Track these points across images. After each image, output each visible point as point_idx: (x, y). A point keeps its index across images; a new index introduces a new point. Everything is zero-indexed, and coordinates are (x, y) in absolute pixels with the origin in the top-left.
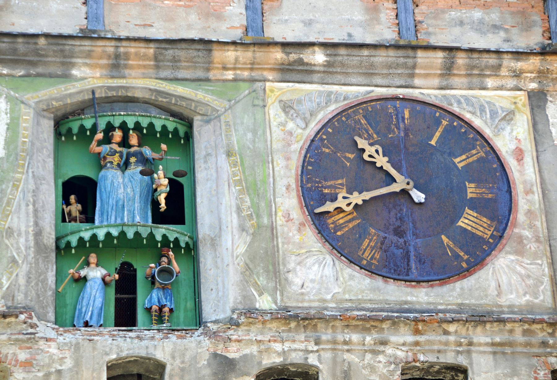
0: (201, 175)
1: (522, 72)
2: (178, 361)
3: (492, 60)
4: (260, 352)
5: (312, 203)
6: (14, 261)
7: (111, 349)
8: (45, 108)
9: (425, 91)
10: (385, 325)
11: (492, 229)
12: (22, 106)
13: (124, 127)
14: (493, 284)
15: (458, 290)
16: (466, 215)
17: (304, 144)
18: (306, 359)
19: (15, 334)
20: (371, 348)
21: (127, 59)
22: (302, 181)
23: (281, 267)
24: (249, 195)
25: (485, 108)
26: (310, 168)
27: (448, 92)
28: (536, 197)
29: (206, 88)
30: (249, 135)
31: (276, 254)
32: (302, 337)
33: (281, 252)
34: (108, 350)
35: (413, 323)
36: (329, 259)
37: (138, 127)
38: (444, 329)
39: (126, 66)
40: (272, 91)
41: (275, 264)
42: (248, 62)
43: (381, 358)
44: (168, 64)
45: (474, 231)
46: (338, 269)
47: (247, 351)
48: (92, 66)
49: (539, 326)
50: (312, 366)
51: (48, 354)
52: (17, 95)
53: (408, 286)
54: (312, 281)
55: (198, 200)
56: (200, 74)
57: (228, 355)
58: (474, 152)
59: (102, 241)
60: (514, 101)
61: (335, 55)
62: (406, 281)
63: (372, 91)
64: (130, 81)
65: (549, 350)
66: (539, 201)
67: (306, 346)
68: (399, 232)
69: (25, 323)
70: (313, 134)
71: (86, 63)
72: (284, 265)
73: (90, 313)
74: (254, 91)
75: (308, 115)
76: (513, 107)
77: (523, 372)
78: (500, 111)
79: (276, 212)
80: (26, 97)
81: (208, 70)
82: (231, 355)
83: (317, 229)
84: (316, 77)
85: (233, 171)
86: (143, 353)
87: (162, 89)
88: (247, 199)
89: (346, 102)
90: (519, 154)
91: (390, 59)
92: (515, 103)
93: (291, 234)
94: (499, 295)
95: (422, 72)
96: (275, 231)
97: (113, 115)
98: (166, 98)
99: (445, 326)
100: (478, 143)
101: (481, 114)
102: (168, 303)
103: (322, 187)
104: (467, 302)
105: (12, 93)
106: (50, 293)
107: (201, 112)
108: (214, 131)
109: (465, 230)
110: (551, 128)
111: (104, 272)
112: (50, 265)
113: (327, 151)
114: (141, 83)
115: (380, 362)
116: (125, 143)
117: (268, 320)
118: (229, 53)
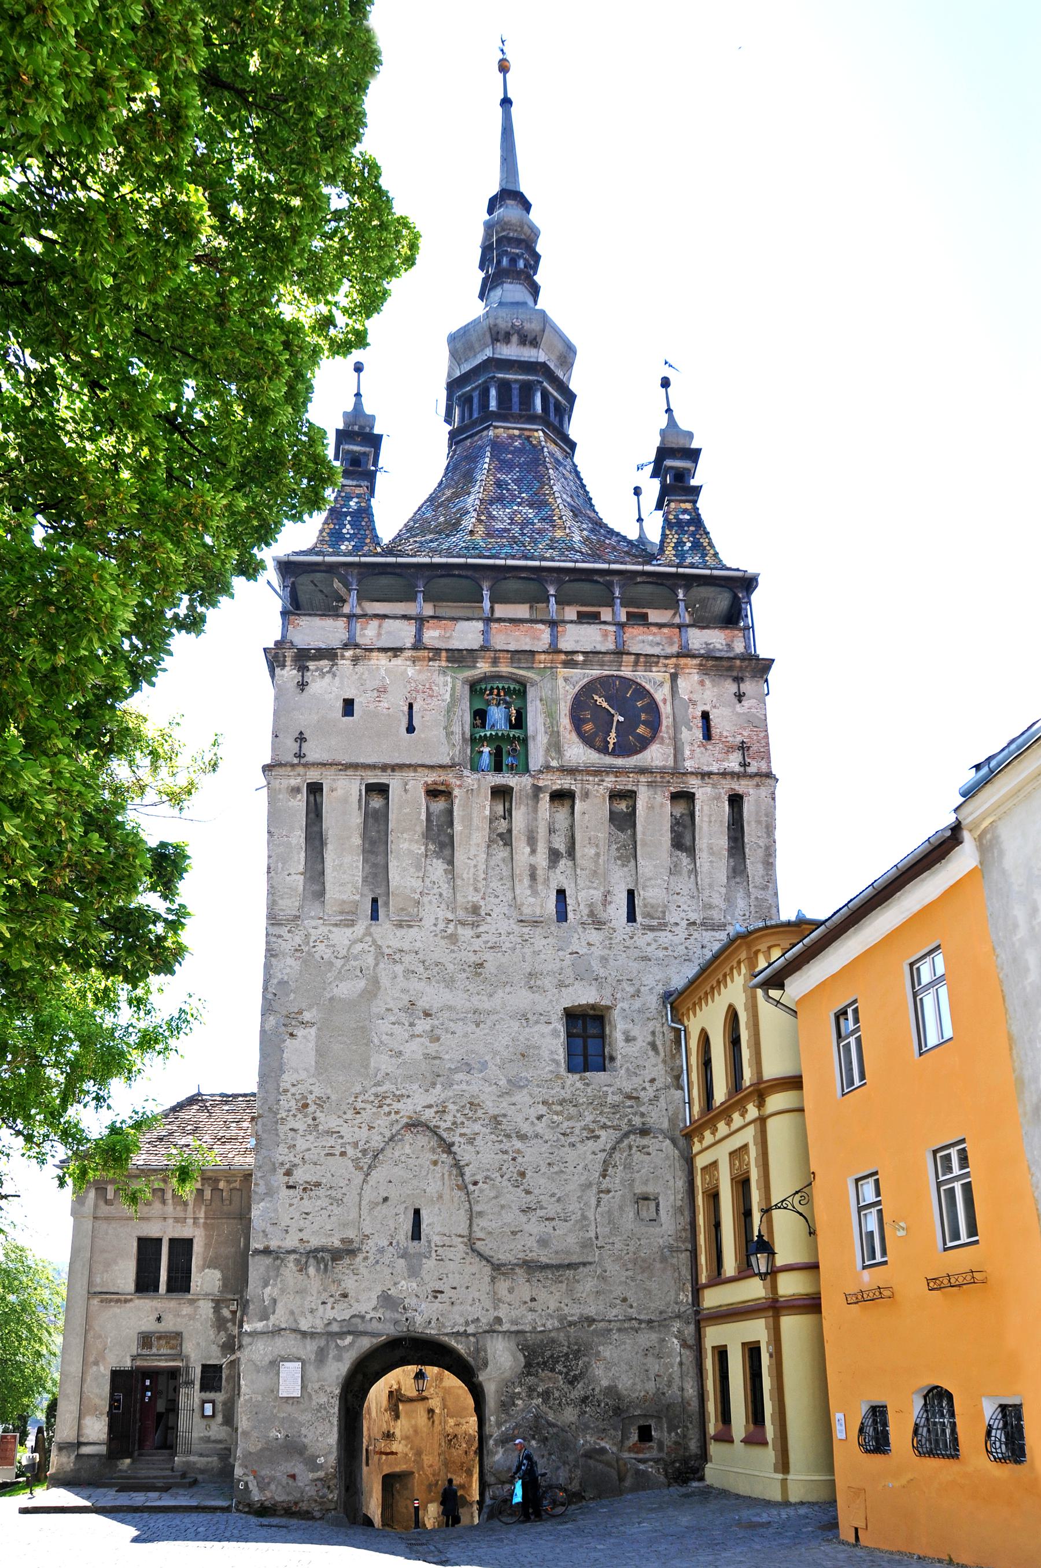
0: (529, 709)
13: (498, 688)
37: (503, 688)
41: (559, 748)
56: (529, 665)
90: (665, 701)
116: (498, 695)
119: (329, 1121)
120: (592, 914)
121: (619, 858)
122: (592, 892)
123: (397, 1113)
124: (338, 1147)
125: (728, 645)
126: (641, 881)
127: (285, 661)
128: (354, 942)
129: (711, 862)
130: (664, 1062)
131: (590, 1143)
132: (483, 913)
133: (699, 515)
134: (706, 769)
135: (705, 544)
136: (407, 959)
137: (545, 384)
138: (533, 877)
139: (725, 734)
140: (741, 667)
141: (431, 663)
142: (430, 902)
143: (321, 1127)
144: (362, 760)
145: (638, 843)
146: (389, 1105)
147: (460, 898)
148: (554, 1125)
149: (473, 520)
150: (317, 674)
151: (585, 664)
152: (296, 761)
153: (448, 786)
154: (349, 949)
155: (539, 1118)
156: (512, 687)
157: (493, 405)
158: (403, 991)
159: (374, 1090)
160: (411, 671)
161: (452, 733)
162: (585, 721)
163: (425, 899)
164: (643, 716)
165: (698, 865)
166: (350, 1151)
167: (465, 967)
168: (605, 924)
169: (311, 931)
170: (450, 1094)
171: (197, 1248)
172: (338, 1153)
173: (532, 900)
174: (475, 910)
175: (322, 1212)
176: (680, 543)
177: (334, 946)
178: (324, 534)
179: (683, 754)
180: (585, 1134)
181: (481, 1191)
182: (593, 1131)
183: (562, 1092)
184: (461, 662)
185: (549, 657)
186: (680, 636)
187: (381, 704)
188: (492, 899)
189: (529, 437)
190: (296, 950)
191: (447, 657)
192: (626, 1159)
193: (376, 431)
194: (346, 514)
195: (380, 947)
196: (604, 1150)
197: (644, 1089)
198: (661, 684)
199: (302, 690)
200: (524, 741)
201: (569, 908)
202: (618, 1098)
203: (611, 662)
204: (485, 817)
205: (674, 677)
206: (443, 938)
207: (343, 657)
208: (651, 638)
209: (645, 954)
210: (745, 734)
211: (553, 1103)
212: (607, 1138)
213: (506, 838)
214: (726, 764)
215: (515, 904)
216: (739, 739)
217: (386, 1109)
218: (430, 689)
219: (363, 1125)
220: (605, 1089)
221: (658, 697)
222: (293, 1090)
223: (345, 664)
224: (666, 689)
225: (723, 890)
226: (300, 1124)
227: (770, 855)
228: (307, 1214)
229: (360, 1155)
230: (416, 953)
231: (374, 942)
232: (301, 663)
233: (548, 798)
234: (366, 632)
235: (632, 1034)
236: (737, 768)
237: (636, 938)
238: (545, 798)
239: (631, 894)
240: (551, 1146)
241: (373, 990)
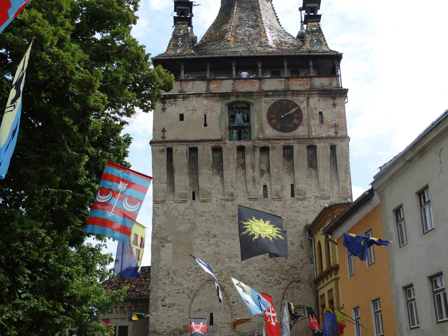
0: (251, 115)
3: (300, 92)
6: (222, 131)
13: (239, 107)
41: (263, 130)
43: (279, 145)
48: (234, 97)
84: (270, 97)
90: (304, 109)
119: (178, 280)
120: (277, 195)
121: (287, 172)
122: (277, 186)
123: (203, 275)
124: (182, 290)
125: (330, 84)
126: (296, 181)
128: (186, 209)
129: (323, 172)
130: (306, 252)
131: (278, 286)
132: (235, 196)
133: (320, 27)
134: (321, 136)
135: (322, 40)
136: (207, 215)
138: (254, 181)
139: (328, 121)
140: (335, 93)
141: (213, 98)
142: (215, 193)
143: (175, 282)
145: (295, 166)
146: (200, 273)
147: (226, 191)
148: (263, 279)
149: (230, 35)
150: (169, 104)
151: (272, 96)
152: (162, 140)
153: (220, 147)
154: (184, 212)
155: (258, 276)
156: (244, 106)
158: (205, 227)
159: (194, 267)
160: (205, 102)
162: (272, 119)
163: (213, 191)
165: (318, 174)
166: (186, 291)
167: (229, 217)
168: (282, 198)
169: (170, 205)
170: (224, 267)
171: (130, 330)
172: (181, 292)
173: (254, 190)
174: (232, 195)
175: (176, 315)
176: (312, 40)
177: (178, 211)
178: (171, 46)
179: (311, 130)
180: (276, 282)
181: (236, 305)
182: (279, 281)
183: (267, 265)
184: (224, 97)
188: (238, 190)
190: (164, 213)
191: (219, 96)
192: (291, 292)
194: (179, 37)
195: (196, 211)
196: (283, 289)
197: (298, 264)
198: (303, 102)
199: (164, 111)
200: (249, 128)
201: (268, 193)
202: (288, 267)
204: (235, 159)
206: (220, 206)
207: (179, 98)
208: (299, 83)
209: (298, 210)
210: (337, 120)
211: (263, 270)
212: (284, 284)
213: (243, 166)
214: (329, 133)
215: (247, 192)
216: (334, 122)
217: (199, 274)
218: (213, 108)
219: (190, 281)
220: (283, 264)
221: (302, 107)
222: (164, 268)
223: (180, 101)
224: (305, 104)
225: (329, 183)
226: (167, 282)
227: (347, 169)
228: (170, 316)
229: (190, 292)
230: (210, 212)
231: (194, 209)
233: (259, 150)
234: (187, 87)
235: (293, 242)
237: (294, 204)
239: (292, 186)
240: (263, 287)
241: (193, 228)
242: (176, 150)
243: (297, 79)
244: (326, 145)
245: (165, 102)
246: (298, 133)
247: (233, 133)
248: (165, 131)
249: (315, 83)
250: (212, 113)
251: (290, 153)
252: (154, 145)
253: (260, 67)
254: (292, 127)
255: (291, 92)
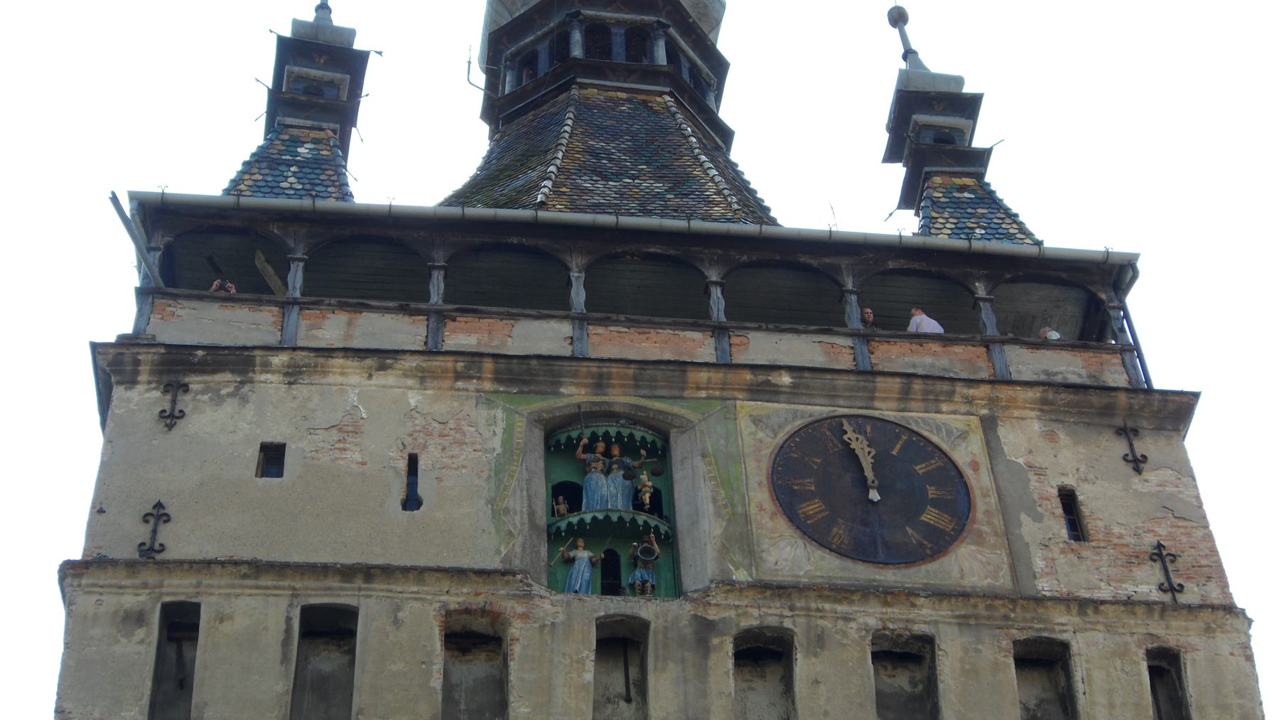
1: (974, 398)
2: (661, 620)
3: (946, 387)
4: (738, 615)
5: (783, 497)
6: (510, 533)
7: (599, 608)
8: (537, 419)
9: (885, 413)
10: (855, 597)
11: (953, 524)
12: (517, 415)
14: (956, 569)
15: (923, 572)
16: (928, 512)
17: (773, 450)
18: (783, 622)
19: (512, 590)
20: (843, 615)
21: (610, 378)
22: (773, 479)
23: (756, 548)
24: (724, 489)
25: (941, 428)
26: (780, 469)
27: (906, 414)
28: (993, 500)
29: (682, 404)
30: (722, 442)
31: (751, 537)
32: (778, 605)
33: (755, 535)
34: (596, 608)
35: (883, 595)
36: (800, 542)
38: (912, 602)
39: (608, 386)
40: (742, 407)
42: (720, 382)
43: (853, 625)
44: (646, 383)
45: (936, 525)
46: (810, 551)
47: (726, 614)
49: (1001, 602)
50: (788, 629)
51: (542, 609)
52: (512, 407)
53: (876, 568)
54: (786, 560)
55: (676, 495)
56: (676, 393)
57: (708, 617)
58: (933, 462)
59: (589, 524)
60: (968, 423)
61: (801, 378)
62: (874, 563)
63: (836, 411)
64: (612, 398)
65: (1010, 623)
66: (996, 503)
67: (781, 612)
68: (865, 523)
69: (521, 582)
70: (781, 442)
71: (572, 382)
72: (758, 546)
73: (579, 584)
74: (726, 407)
75: (776, 427)
76: (967, 428)
77: (987, 641)
78: (955, 431)
79: (749, 503)
80: (520, 408)
81: (683, 389)
82: (711, 618)
83: (788, 517)
84: (783, 397)
85: (708, 470)
86: (629, 612)
87: (641, 404)
88: (722, 492)
89: (811, 419)
91: (852, 383)
92: (969, 425)
93: (764, 521)
94: (962, 577)
95: (882, 395)
96: (749, 518)
97: (597, 426)
98: (644, 412)
99: (912, 599)
100: (936, 455)
101: (938, 432)
102: (650, 580)
103: (792, 484)
104: (932, 582)
105: (508, 406)
106: (543, 564)
107: (676, 425)
108: (690, 439)
109: (929, 524)
110: (1003, 446)
111: (591, 554)
112: (543, 543)
113: (795, 456)
114: (622, 399)
115: (851, 628)
116: (607, 453)
117: (745, 588)
118: (702, 374)
127: (136, 373)
134: (1085, 594)
135: (1012, 231)
137: (672, 31)
139: (1116, 530)
140: (1130, 408)
141: (460, 384)
144: (296, 558)
150: (206, 397)
151: (794, 393)
157: (577, 51)
160: (413, 399)
161: (507, 511)
162: (806, 497)
164: (932, 492)
178: (242, 187)
179: (1029, 565)
184: (525, 382)
185: (717, 376)
186: (990, 359)
187: (348, 454)
189: (645, 103)
193: (358, 45)
198: (963, 436)
199: (170, 427)
200: (670, 541)
203: (851, 389)
205: (989, 425)
207: (266, 367)
216: (1149, 540)
218: (458, 429)
223: (269, 383)
232: (172, 378)
233: (729, 648)
236: (1156, 596)
238: (724, 650)
242: (221, 619)
243: (914, 347)
244: (1126, 644)
245: (185, 388)
246: (955, 573)
247: (570, 561)
248: (168, 519)
249: (1011, 369)
250: (455, 450)
251: (908, 688)
252: (84, 581)
253: (716, 283)
254: (921, 545)
255: (896, 383)
